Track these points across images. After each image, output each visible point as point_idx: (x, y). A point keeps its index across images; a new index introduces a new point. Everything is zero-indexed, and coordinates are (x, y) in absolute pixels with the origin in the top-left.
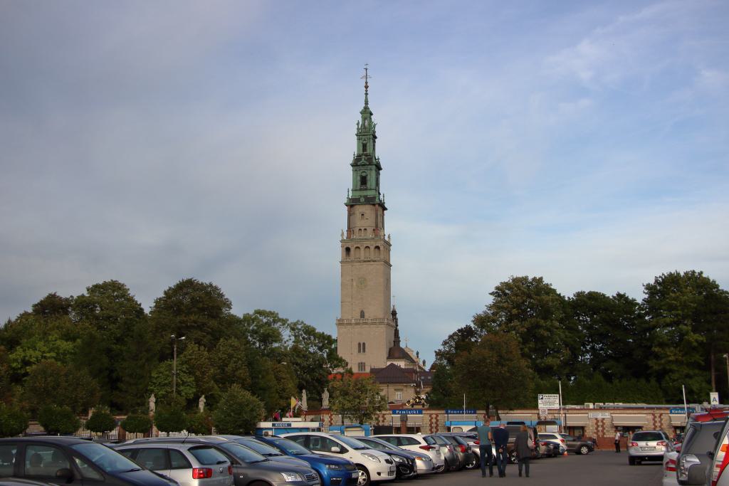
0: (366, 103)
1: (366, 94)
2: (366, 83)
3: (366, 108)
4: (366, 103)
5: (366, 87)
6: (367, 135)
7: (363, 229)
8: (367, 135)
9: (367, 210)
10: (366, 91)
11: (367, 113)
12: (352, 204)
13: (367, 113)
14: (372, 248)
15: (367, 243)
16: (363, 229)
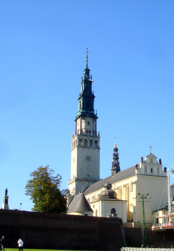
0: (87, 66)
1: (87, 61)
2: (87, 55)
3: (87, 68)
4: (87, 66)
5: (87, 57)
6: (88, 83)
7: (88, 130)
8: (88, 83)
9: (90, 120)
10: (87, 59)
11: (87, 71)
12: (83, 116)
13: (87, 71)
14: (94, 142)
15: (92, 139)
16: (88, 130)
